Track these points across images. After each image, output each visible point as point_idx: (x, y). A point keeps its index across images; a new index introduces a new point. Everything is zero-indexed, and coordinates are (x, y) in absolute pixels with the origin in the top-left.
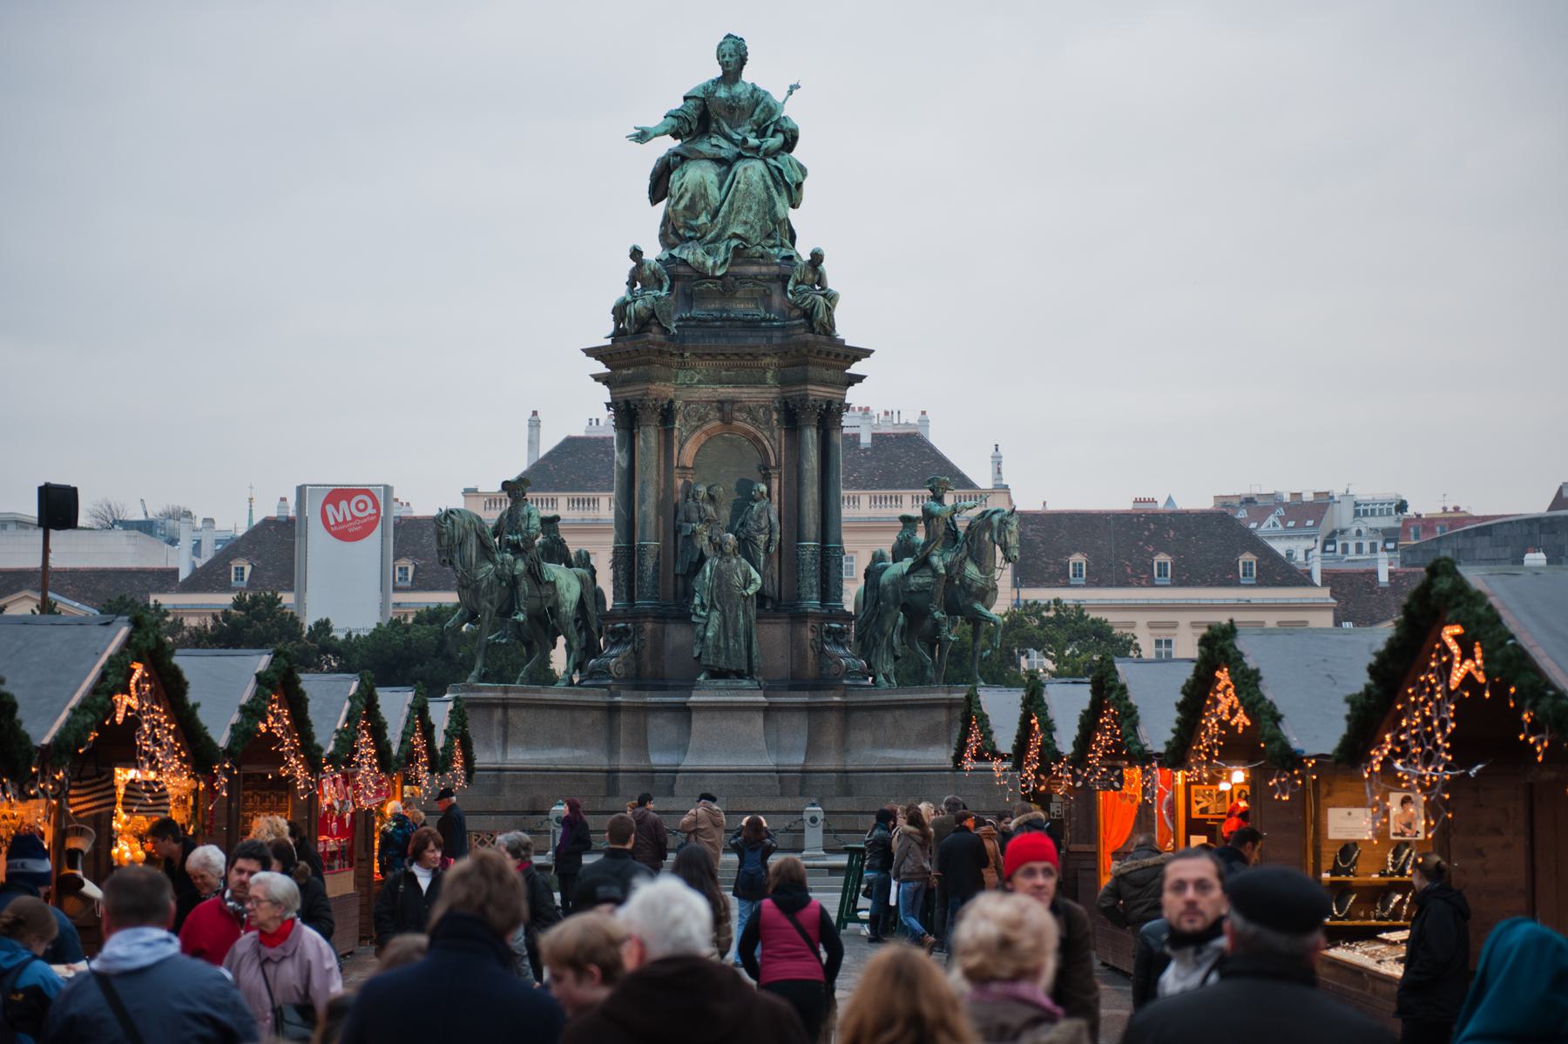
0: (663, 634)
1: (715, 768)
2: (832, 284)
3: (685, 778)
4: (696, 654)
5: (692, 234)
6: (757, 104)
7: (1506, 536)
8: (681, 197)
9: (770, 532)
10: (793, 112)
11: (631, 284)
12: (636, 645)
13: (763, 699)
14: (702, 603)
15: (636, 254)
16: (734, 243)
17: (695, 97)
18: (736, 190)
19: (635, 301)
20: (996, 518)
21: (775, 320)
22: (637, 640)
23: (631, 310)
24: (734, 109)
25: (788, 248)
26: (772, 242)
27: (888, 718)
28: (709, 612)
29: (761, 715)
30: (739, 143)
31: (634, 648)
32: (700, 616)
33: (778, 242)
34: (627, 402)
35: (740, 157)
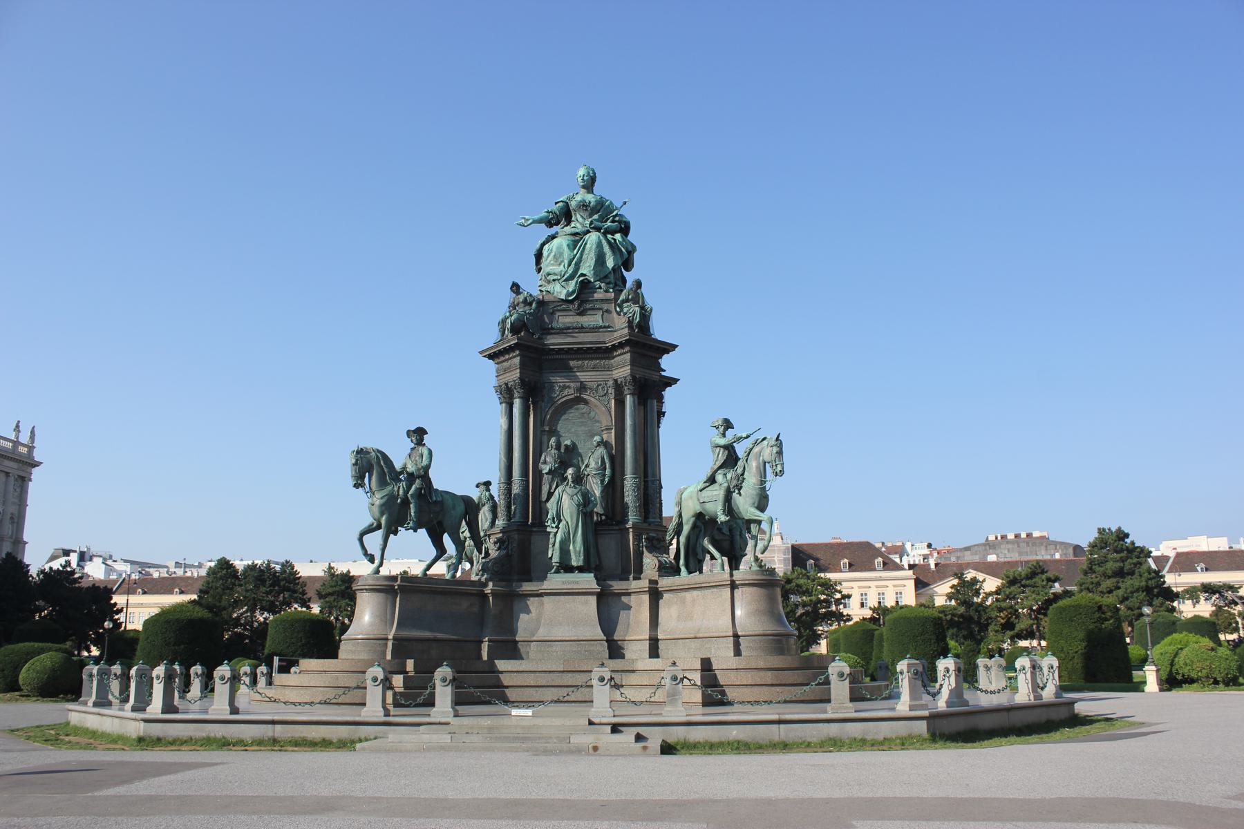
0: (530, 544)
1: (560, 639)
2: (650, 301)
3: (537, 646)
4: (550, 556)
5: (556, 277)
6: (602, 206)
7: (976, 551)
8: (548, 256)
9: (605, 469)
10: (627, 213)
11: (514, 306)
12: (510, 552)
13: (597, 586)
14: (554, 518)
15: (516, 288)
16: (581, 278)
17: (562, 201)
18: (584, 249)
19: (511, 316)
20: (765, 442)
21: (609, 327)
22: (510, 548)
23: (509, 321)
24: (587, 206)
25: (619, 286)
26: (607, 281)
27: (689, 596)
28: (559, 524)
29: (595, 597)
30: (588, 225)
31: (507, 553)
32: (553, 527)
33: (613, 281)
34: (506, 384)
35: (588, 232)
